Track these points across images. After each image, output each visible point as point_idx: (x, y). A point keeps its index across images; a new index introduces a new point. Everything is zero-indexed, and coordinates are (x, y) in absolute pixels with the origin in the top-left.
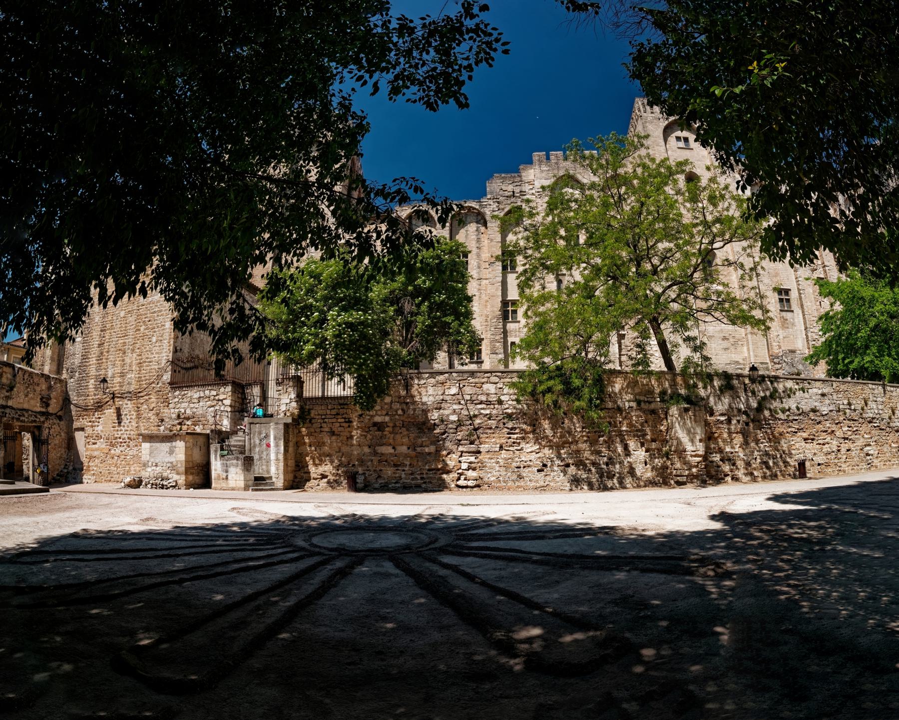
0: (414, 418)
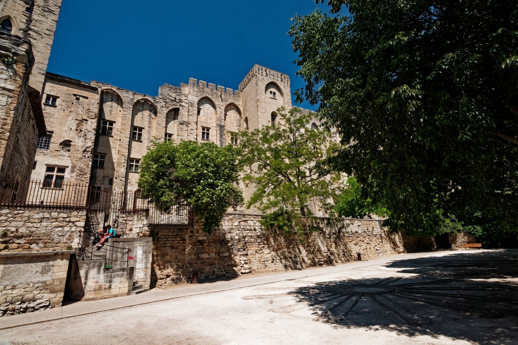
0: (219, 238)
